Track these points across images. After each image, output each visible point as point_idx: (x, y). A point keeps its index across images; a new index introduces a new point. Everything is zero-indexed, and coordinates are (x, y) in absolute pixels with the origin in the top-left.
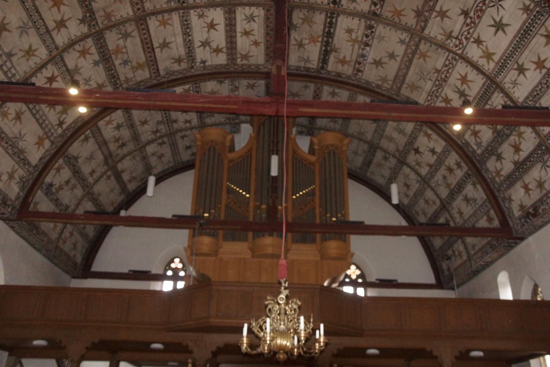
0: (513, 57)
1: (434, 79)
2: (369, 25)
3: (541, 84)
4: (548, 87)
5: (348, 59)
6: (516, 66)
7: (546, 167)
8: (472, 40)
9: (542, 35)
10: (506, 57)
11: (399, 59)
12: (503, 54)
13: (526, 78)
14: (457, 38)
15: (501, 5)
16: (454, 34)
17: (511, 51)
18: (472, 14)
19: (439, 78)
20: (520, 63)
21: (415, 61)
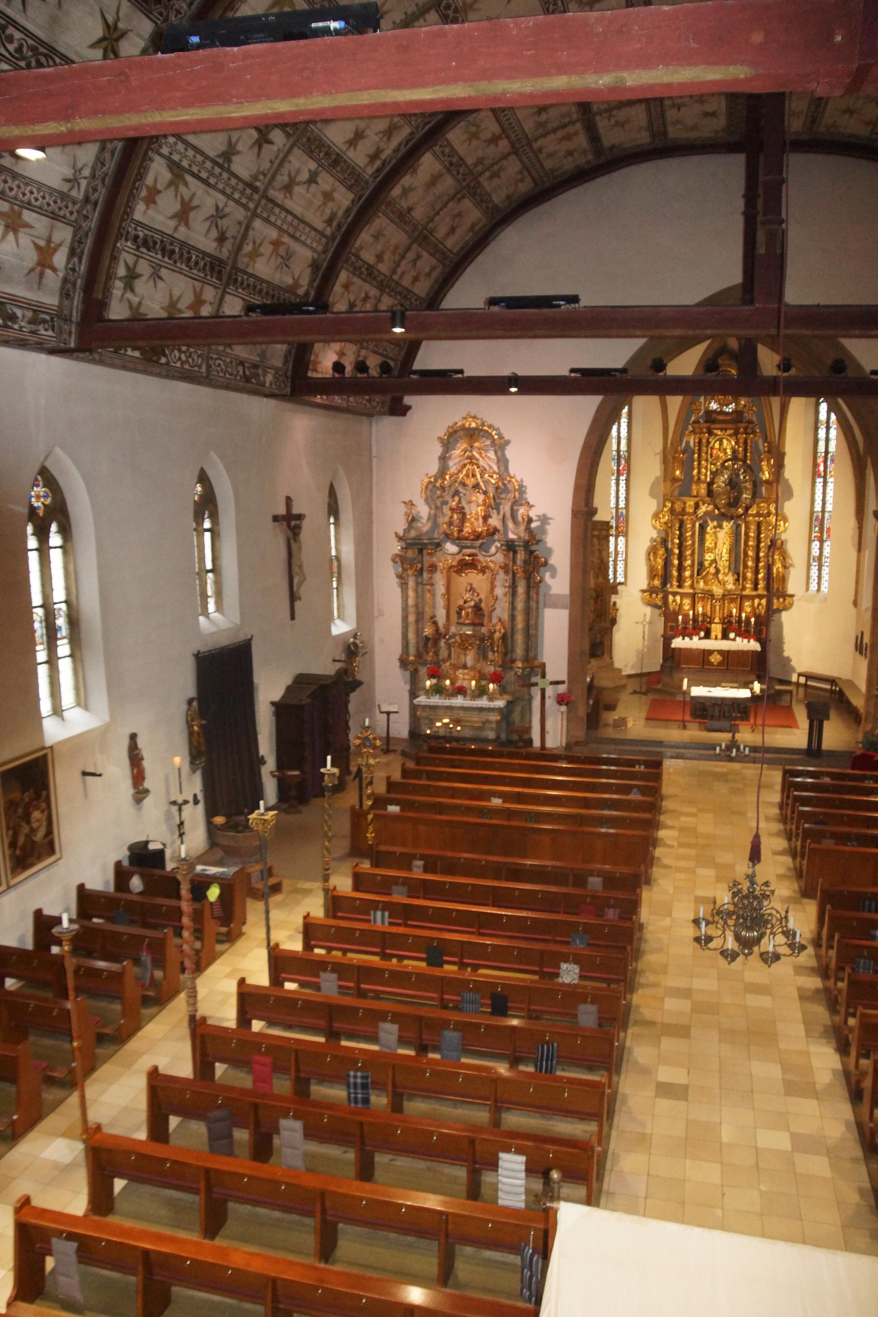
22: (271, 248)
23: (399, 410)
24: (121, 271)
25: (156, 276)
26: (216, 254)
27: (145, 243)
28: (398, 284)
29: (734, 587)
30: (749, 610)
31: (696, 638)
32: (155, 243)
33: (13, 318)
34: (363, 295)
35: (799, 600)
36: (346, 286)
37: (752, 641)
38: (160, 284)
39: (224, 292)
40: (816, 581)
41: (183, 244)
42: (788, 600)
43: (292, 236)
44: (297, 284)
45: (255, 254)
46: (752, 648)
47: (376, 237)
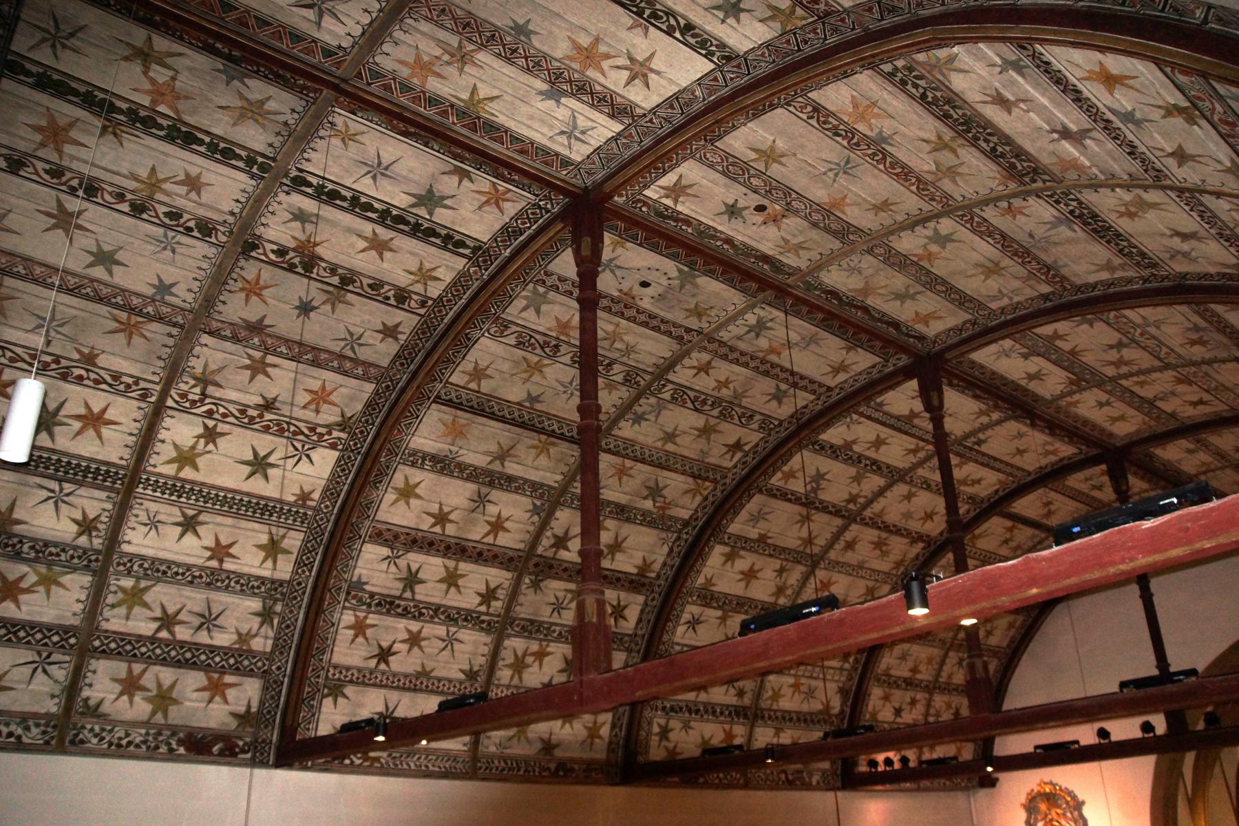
0: (205, 502)
1: (55, 349)
2: (217, 230)
3: (188, 570)
4: (191, 582)
5: (69, 149)
6: (191, 513)
7: (40, 669)
8: (211, 423)
9: (270, 533)
10: (200, 491)
11: (99, 272)
12: (202, 484)
13: (179, 539)
14: (204, 395)
15: (300, 459)
16: (211, 390)
17: (217, 495)
18: (268, 416)
19: (64, 363)
20: (202, 518)
21: (103, 310)
22: (791, 690)
23: (989, 782)
24: (656, 729)
25: (686, 727)
26: (740, 703)
27: (672, 709)
28: (949, 684)
32: (681, 709)
33: (572, 770)
34: (909, 700)
36: (886, 698)
38: (690, 732)
39: (752, 727)
41: (705, 704)
43: (811, 677)
44: (827, 707)
45: (776, 696)
47: (903, 658)
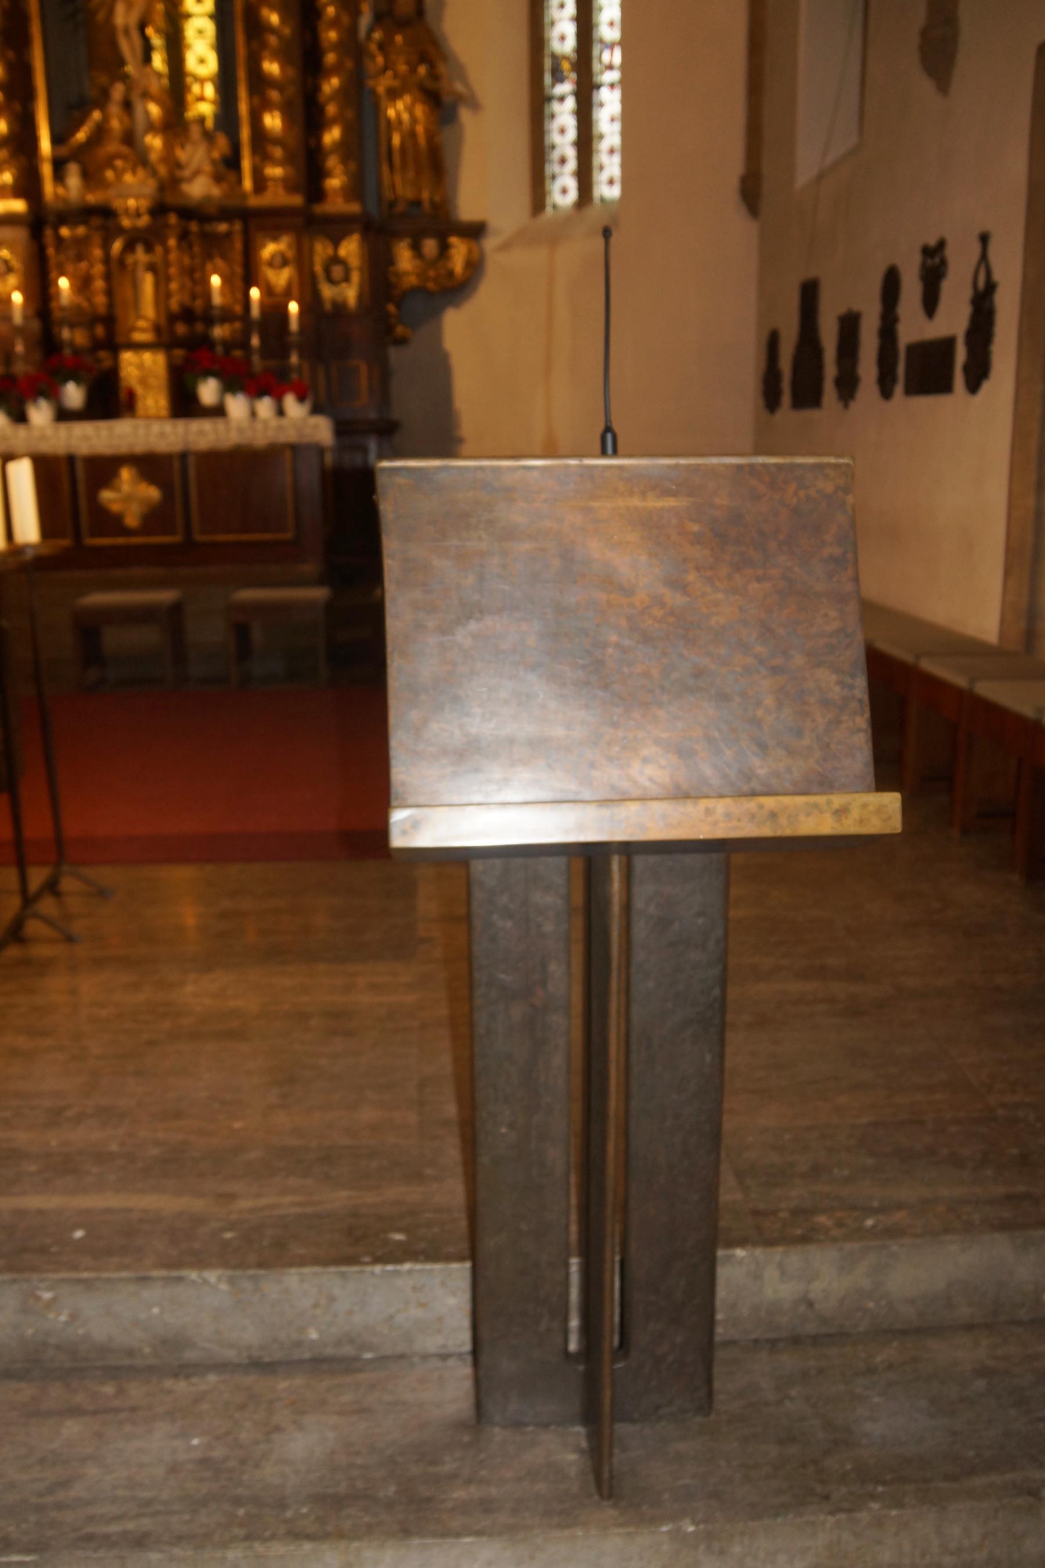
29: (216, 191)
30: (281, 278)
31: (40, 414)
35: (505, 247)
37: (290, 402)
40: (572, 165)
42: (459, 251)
46: (290, 436)
